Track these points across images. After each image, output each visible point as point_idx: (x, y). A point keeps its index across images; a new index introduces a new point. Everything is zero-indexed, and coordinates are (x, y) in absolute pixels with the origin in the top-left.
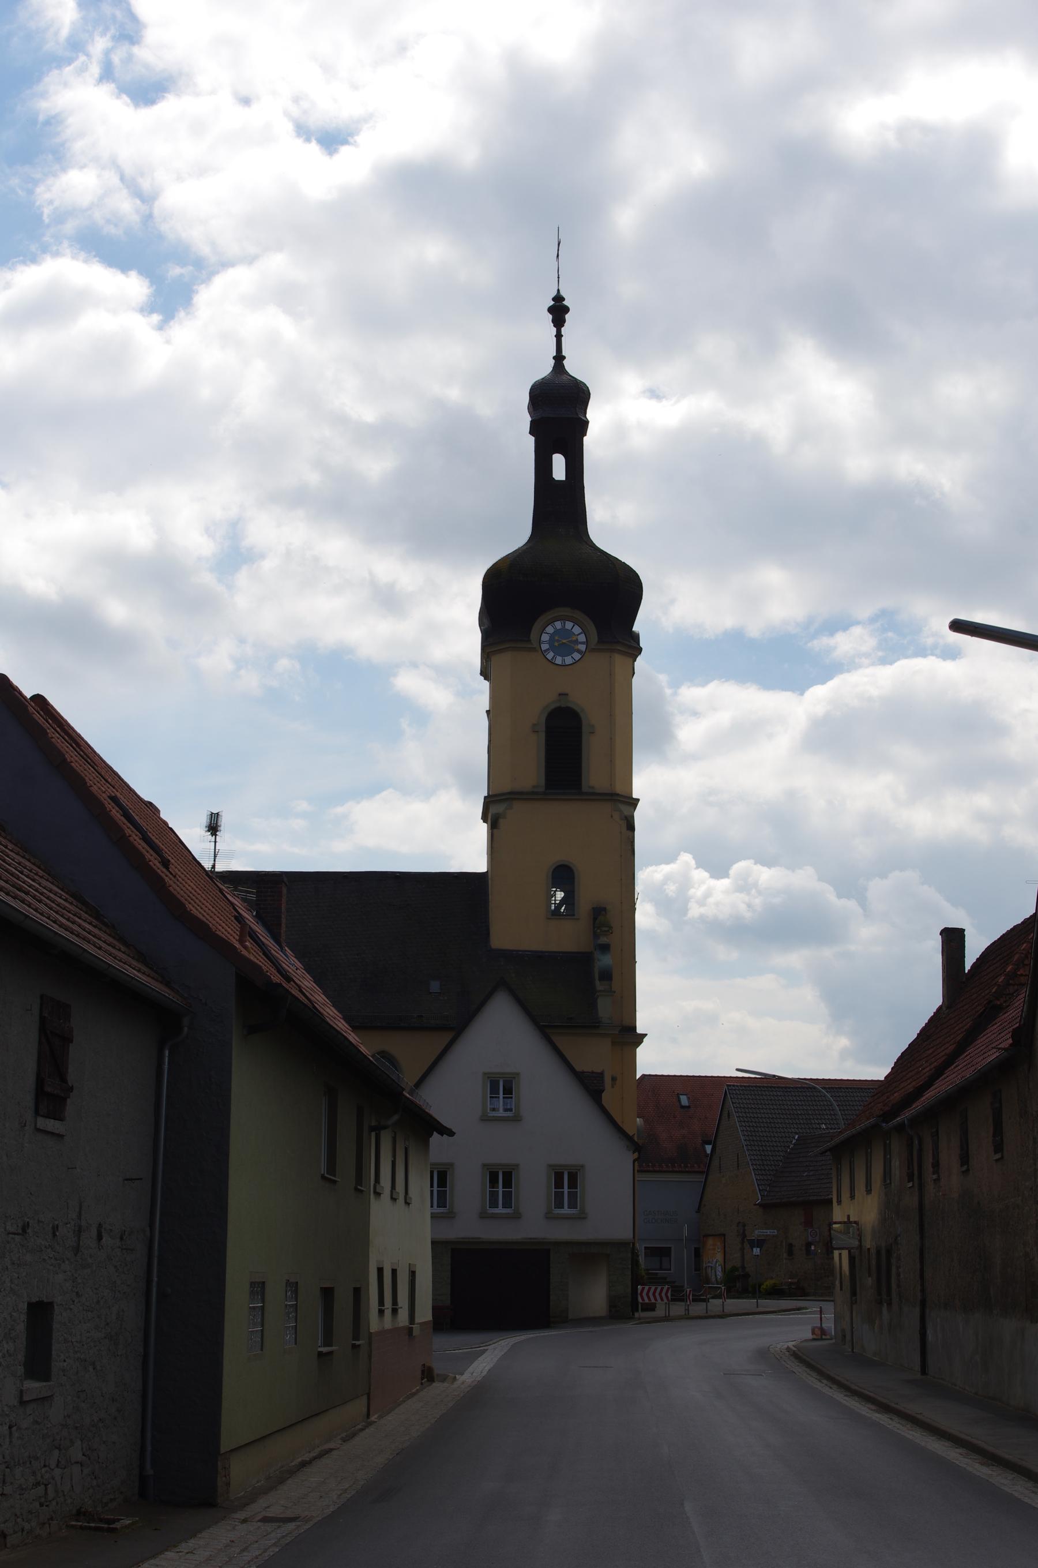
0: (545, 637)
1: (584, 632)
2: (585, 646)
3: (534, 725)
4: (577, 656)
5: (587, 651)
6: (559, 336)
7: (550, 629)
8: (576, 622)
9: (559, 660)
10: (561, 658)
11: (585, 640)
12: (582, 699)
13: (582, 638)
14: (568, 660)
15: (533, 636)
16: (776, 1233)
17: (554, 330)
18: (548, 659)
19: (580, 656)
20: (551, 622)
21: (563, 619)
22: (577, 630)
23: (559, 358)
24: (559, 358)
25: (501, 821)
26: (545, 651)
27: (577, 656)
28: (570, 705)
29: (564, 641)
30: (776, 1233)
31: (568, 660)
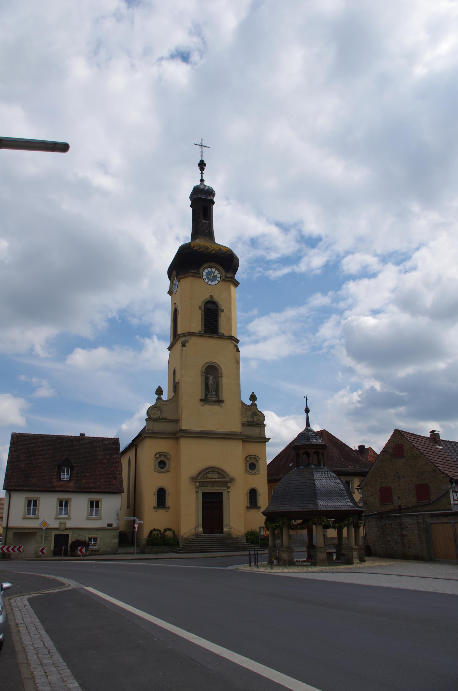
0: (204, 273)
1: (219, 273)
2: (220, 279)
3: (200, 307)
4: (217, 282)
5: (221, 281)
6: (202, 173)
7: (206, 271)
8: (216, 269)
9: (210, 283)
10: (210, 282)
11: (220, 276)
12: (219, 299)
13: (219, 275)
14: (213, 283)
15: (201, 270)
16: (142, 523)
17: (201, 172)
18: (205, 282)
19: (218, 282)
20: (207, 268)
21: (212, 267)
22: (217, 272)
23: (202, 181)
24: (202, 181)
25: (187, 343)
26: (205, 278)
27: (217, 282)
28: (213, 300)
29: (212, 275)
30: (142, 523)
31: (213, 283)
